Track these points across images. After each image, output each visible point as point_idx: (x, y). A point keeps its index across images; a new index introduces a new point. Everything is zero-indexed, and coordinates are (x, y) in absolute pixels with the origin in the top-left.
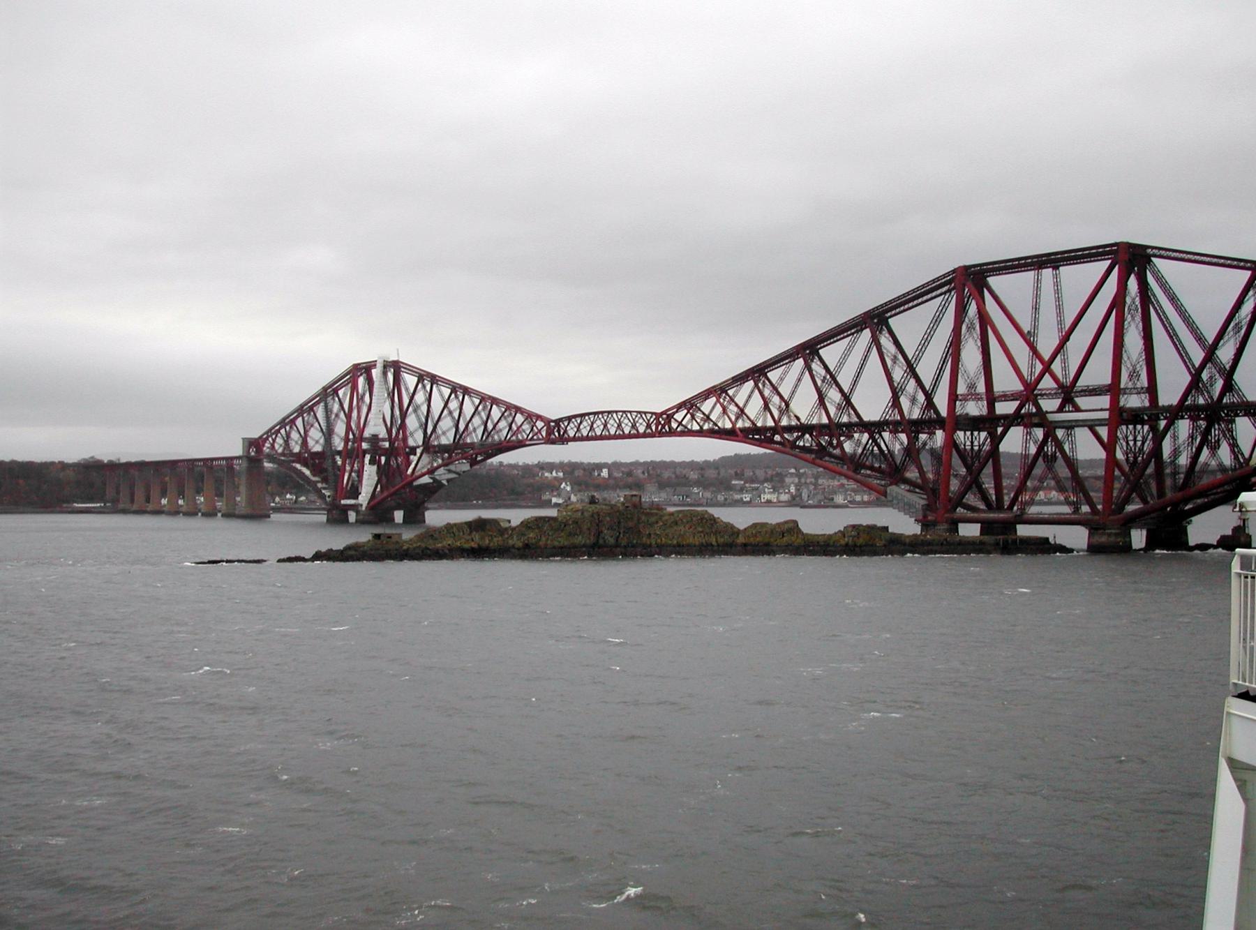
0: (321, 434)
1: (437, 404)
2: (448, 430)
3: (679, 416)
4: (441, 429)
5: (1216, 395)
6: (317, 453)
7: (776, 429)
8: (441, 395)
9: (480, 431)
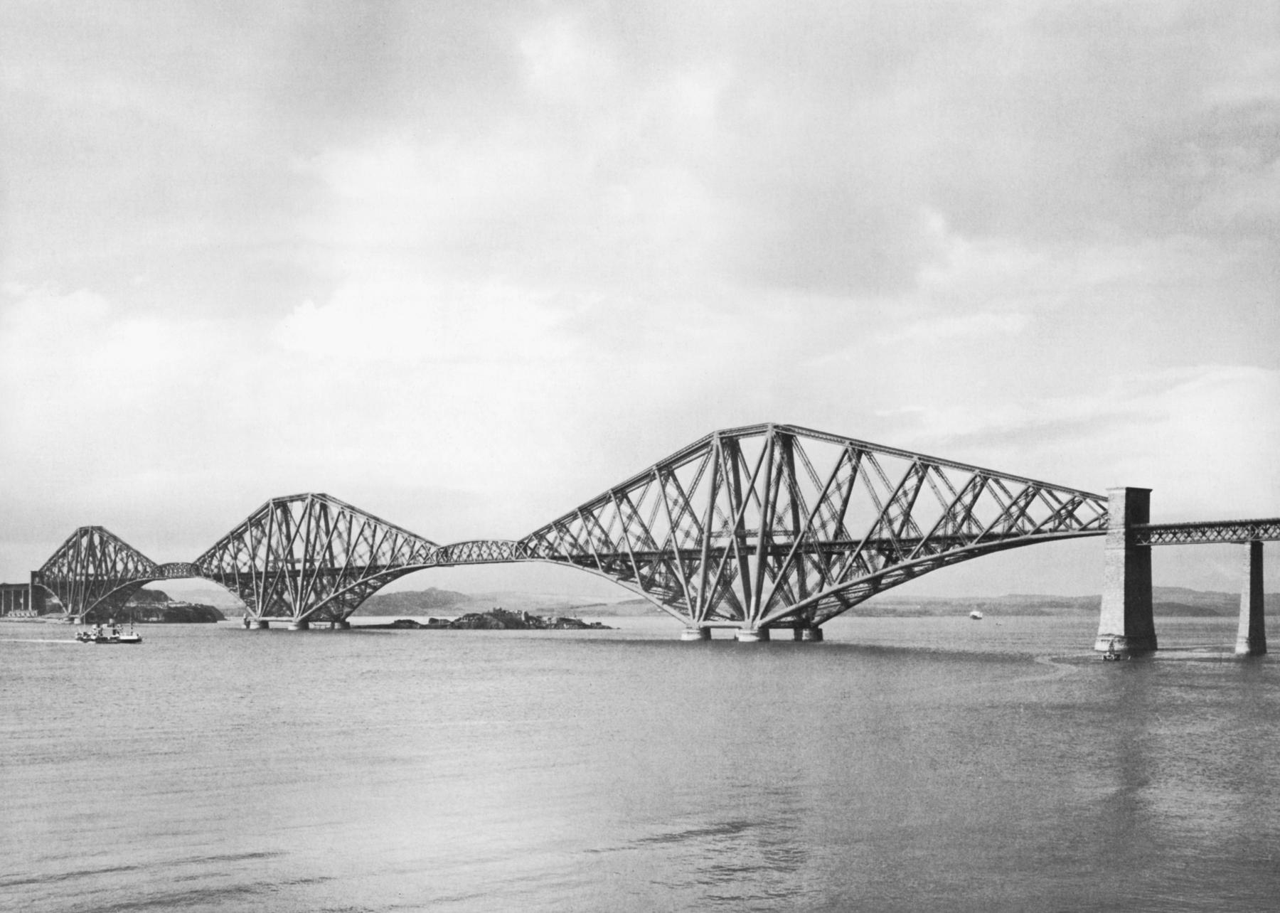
1: (356, 530)
3: (532, 545)
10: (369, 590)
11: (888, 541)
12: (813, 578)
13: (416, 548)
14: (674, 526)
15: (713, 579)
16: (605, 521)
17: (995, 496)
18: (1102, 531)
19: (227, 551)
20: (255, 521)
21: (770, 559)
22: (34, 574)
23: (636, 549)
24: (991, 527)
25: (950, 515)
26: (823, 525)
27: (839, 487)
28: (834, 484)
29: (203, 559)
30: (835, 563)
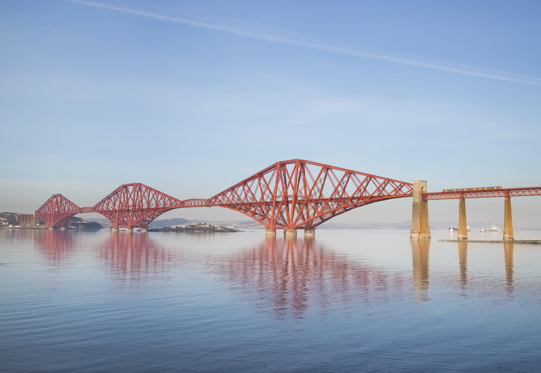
0: (112, 205)
1: (151, 196)
2: (154, 204)
3: (213, 200)
4: (151, 203)
5: (341, 195)
6: (111, 211)
8: (152, 193)
9: (162, 204)
10: (155, 216)
11: (336, 199)
12: (312, 212)
13: (172, 202)
14: (263, 194)
15: (276, 212)
16: (239, 193)
17: (374, 183)
18: (411, 195)
19: (105, 203)
20: (115, 193)
21: (297, 205)
23: (250, 202)
24: (373, 194)
25: (359, 189)
26: (315, 194)
27: (321, 180)
28: (319, 180)
30: (319, 207)
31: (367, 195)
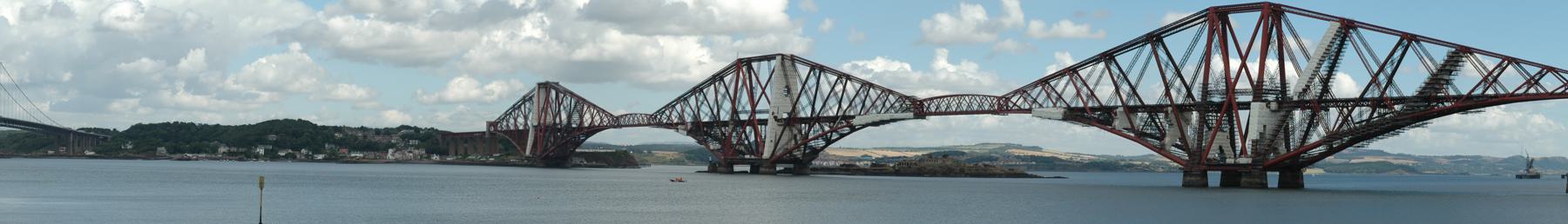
1: (825, 88)
7: (1083, 110)
11: (1373, 100)
22: (490, 124)
29: (662, 112)
31: (1452, 92)
